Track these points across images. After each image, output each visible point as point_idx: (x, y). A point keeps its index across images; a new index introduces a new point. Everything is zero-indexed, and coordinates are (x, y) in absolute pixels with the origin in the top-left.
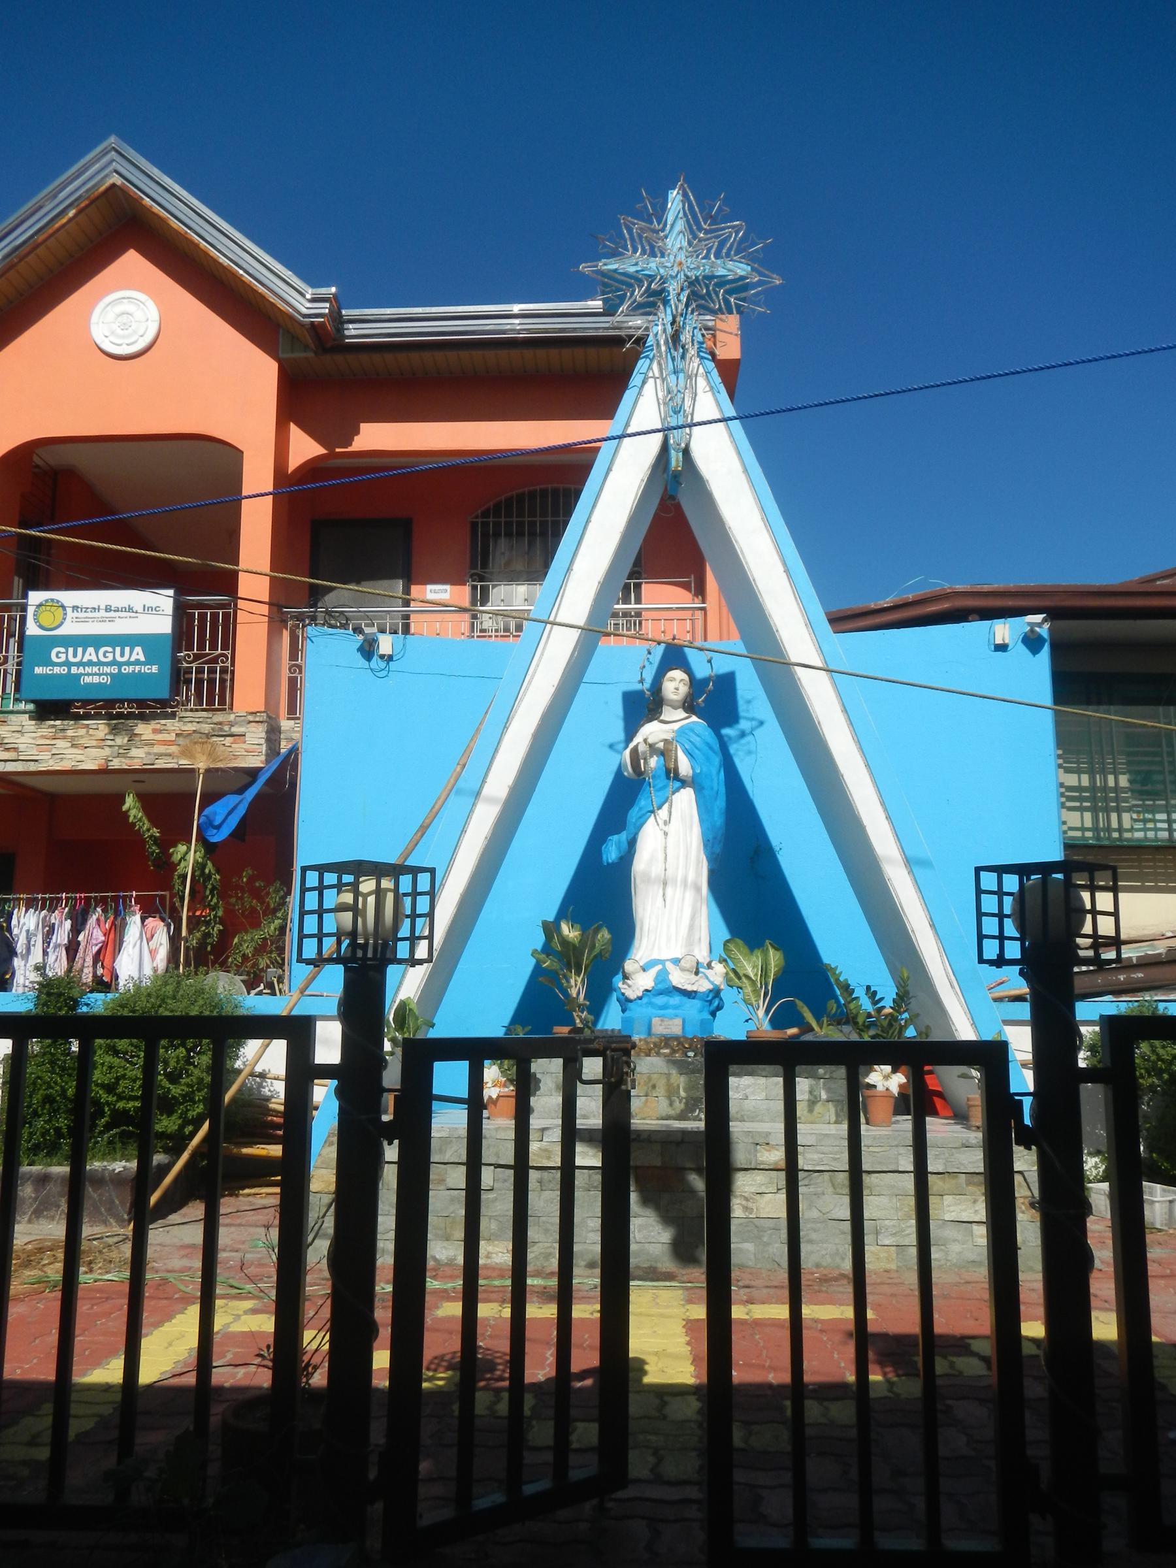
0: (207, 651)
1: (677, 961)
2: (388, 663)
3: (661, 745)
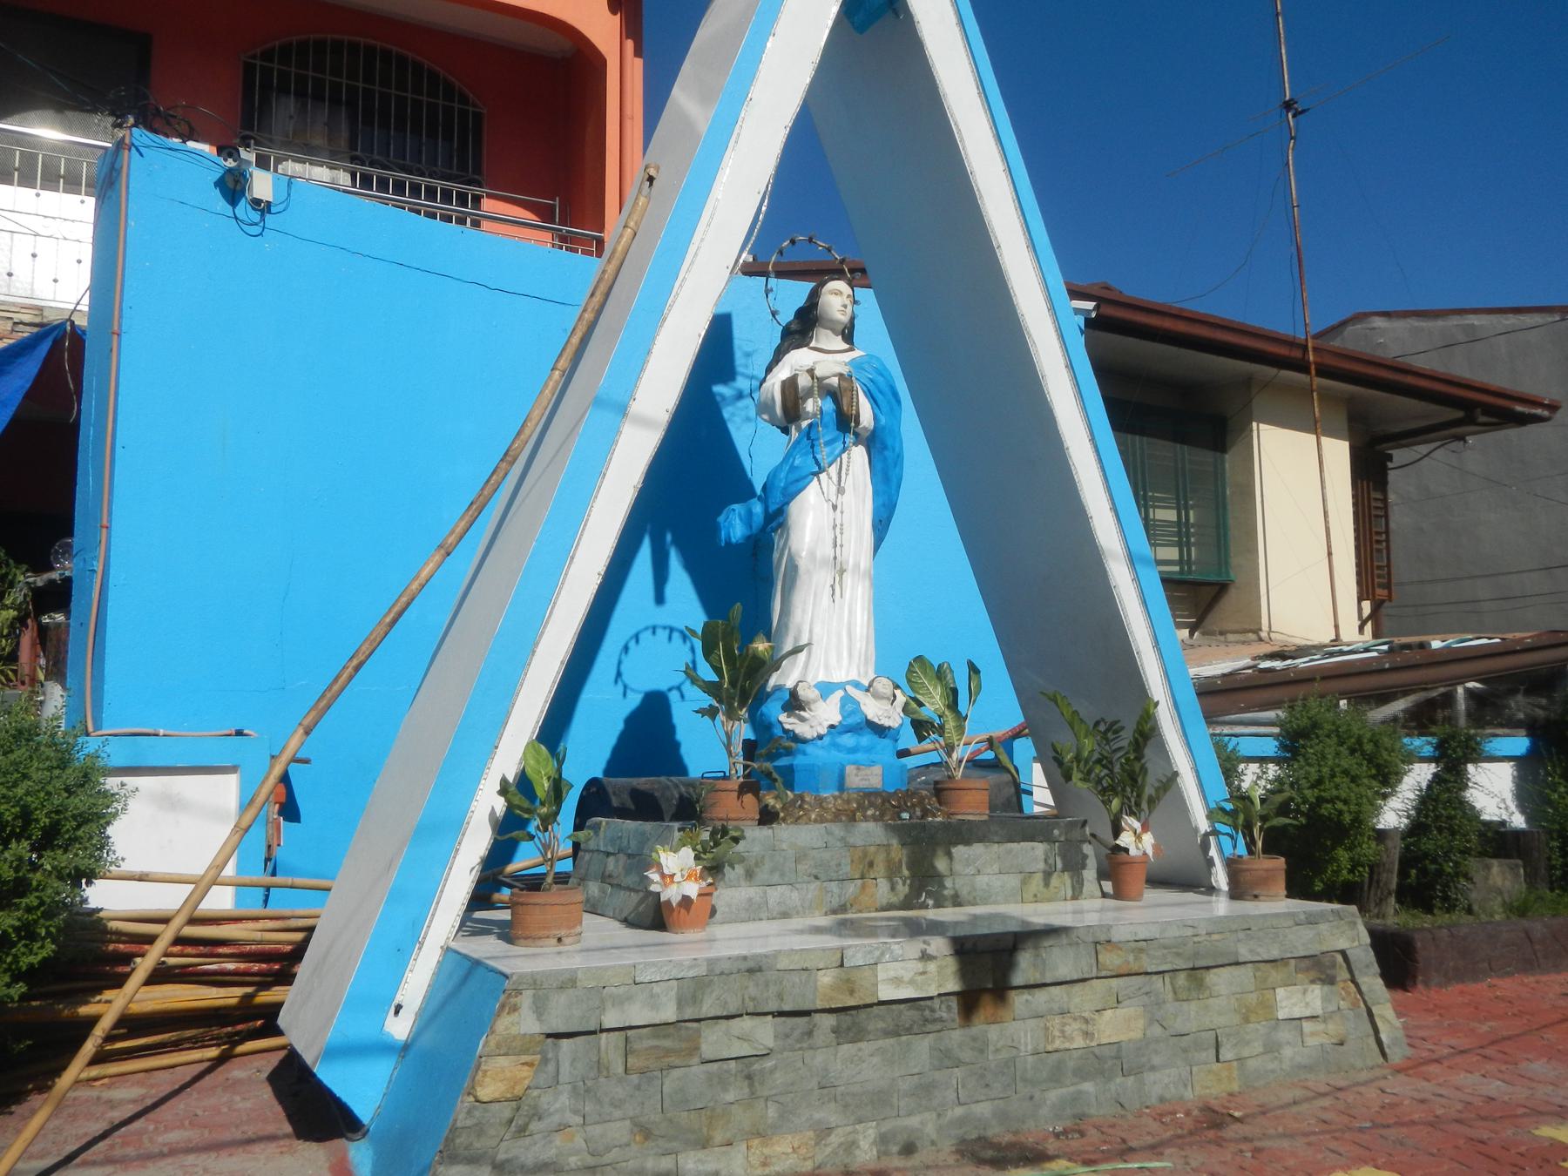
2: (262, 216)
3: (835, 381)
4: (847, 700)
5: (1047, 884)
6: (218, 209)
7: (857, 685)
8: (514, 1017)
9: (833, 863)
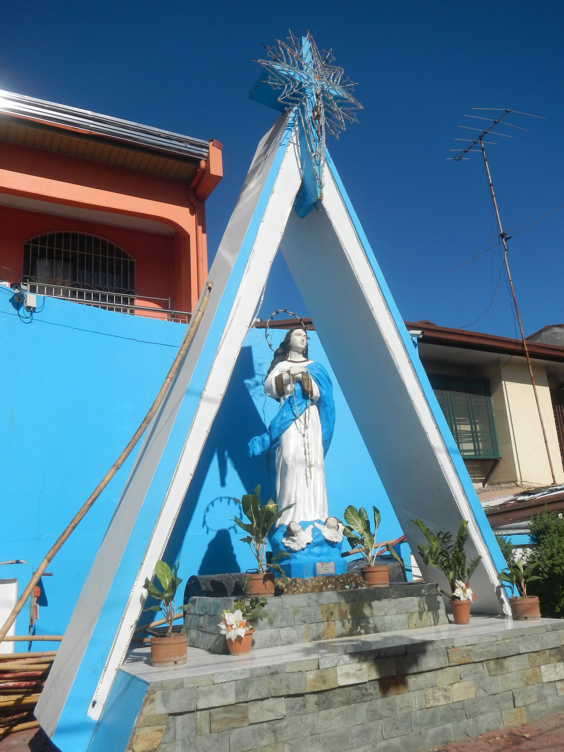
2: (31, 314)
3: (300, 376)
4: (315, 530)
5: (421, 618)
6: (11, 312)
7: (319, 522)
8: (152, 705)
9: (313, 614)
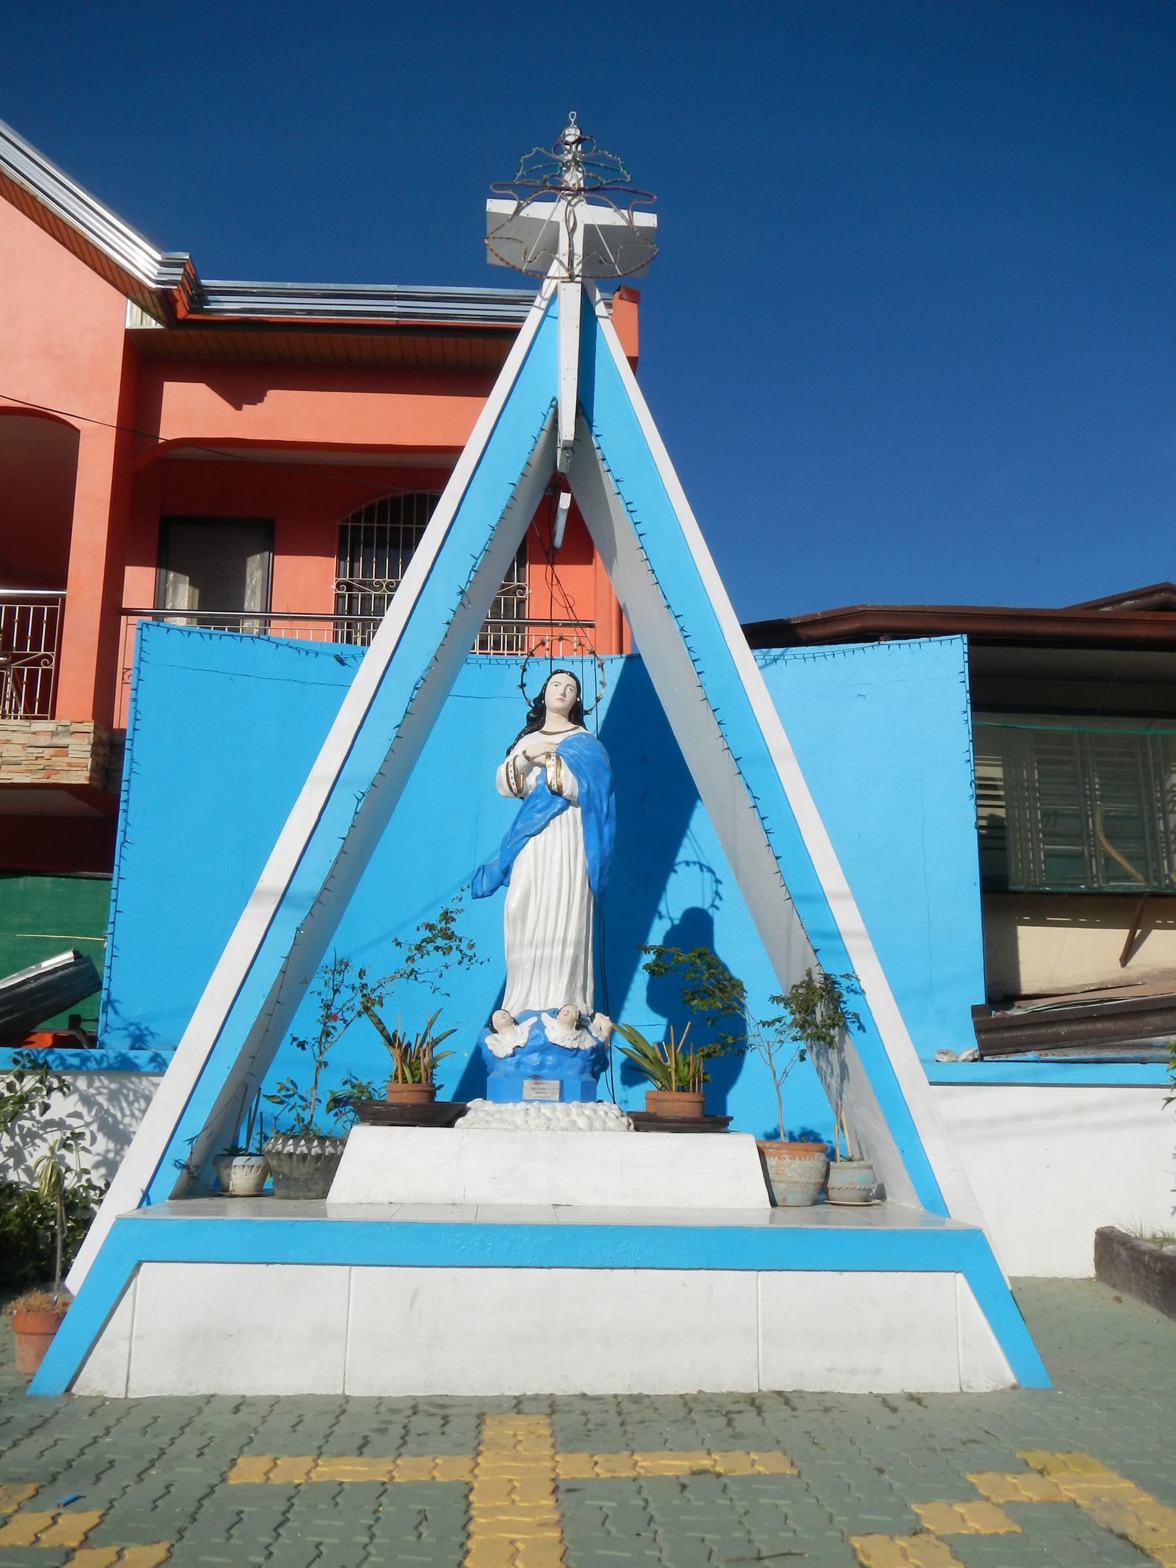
0: (28, 651)
1: (555, 1013)
